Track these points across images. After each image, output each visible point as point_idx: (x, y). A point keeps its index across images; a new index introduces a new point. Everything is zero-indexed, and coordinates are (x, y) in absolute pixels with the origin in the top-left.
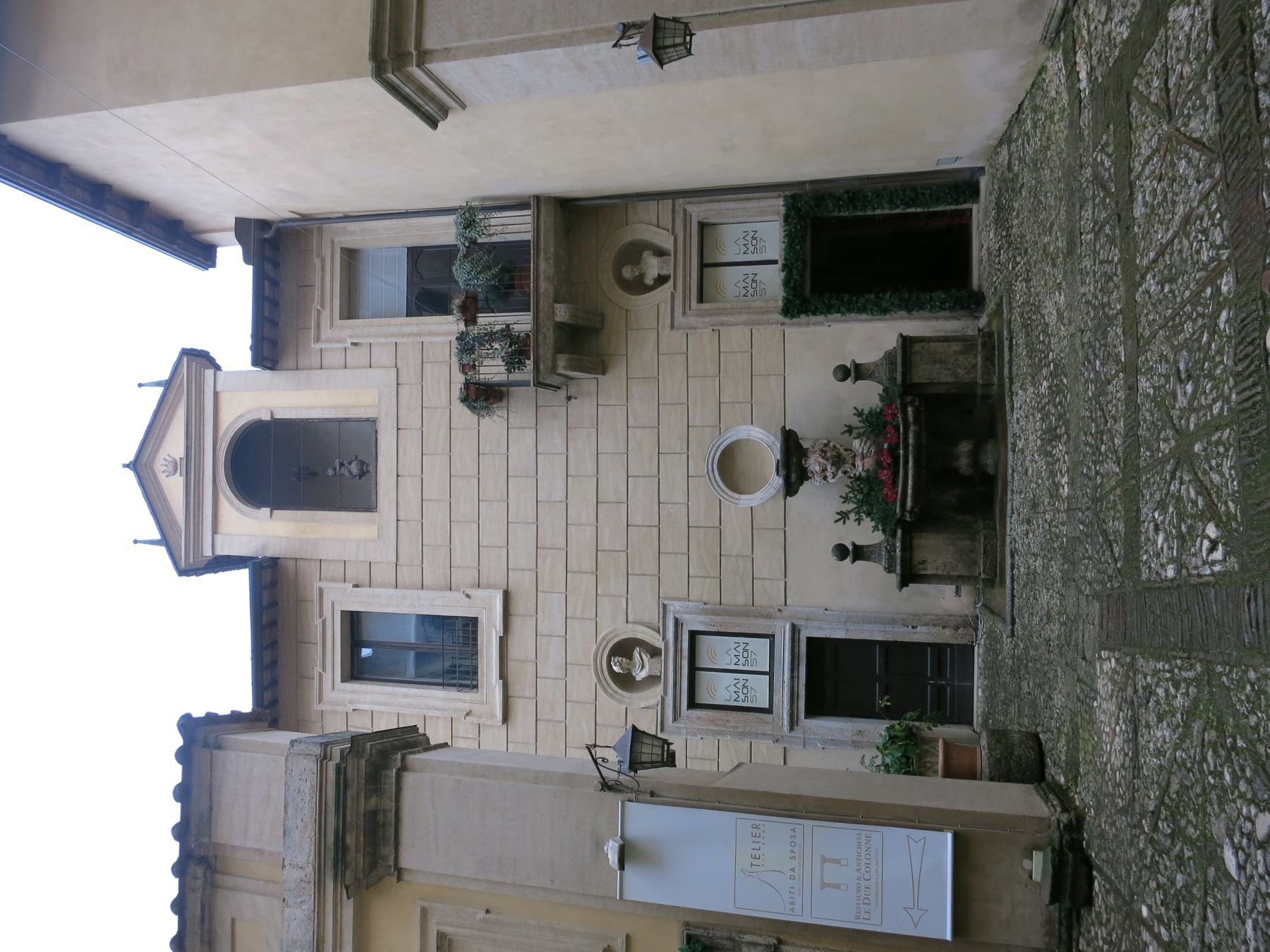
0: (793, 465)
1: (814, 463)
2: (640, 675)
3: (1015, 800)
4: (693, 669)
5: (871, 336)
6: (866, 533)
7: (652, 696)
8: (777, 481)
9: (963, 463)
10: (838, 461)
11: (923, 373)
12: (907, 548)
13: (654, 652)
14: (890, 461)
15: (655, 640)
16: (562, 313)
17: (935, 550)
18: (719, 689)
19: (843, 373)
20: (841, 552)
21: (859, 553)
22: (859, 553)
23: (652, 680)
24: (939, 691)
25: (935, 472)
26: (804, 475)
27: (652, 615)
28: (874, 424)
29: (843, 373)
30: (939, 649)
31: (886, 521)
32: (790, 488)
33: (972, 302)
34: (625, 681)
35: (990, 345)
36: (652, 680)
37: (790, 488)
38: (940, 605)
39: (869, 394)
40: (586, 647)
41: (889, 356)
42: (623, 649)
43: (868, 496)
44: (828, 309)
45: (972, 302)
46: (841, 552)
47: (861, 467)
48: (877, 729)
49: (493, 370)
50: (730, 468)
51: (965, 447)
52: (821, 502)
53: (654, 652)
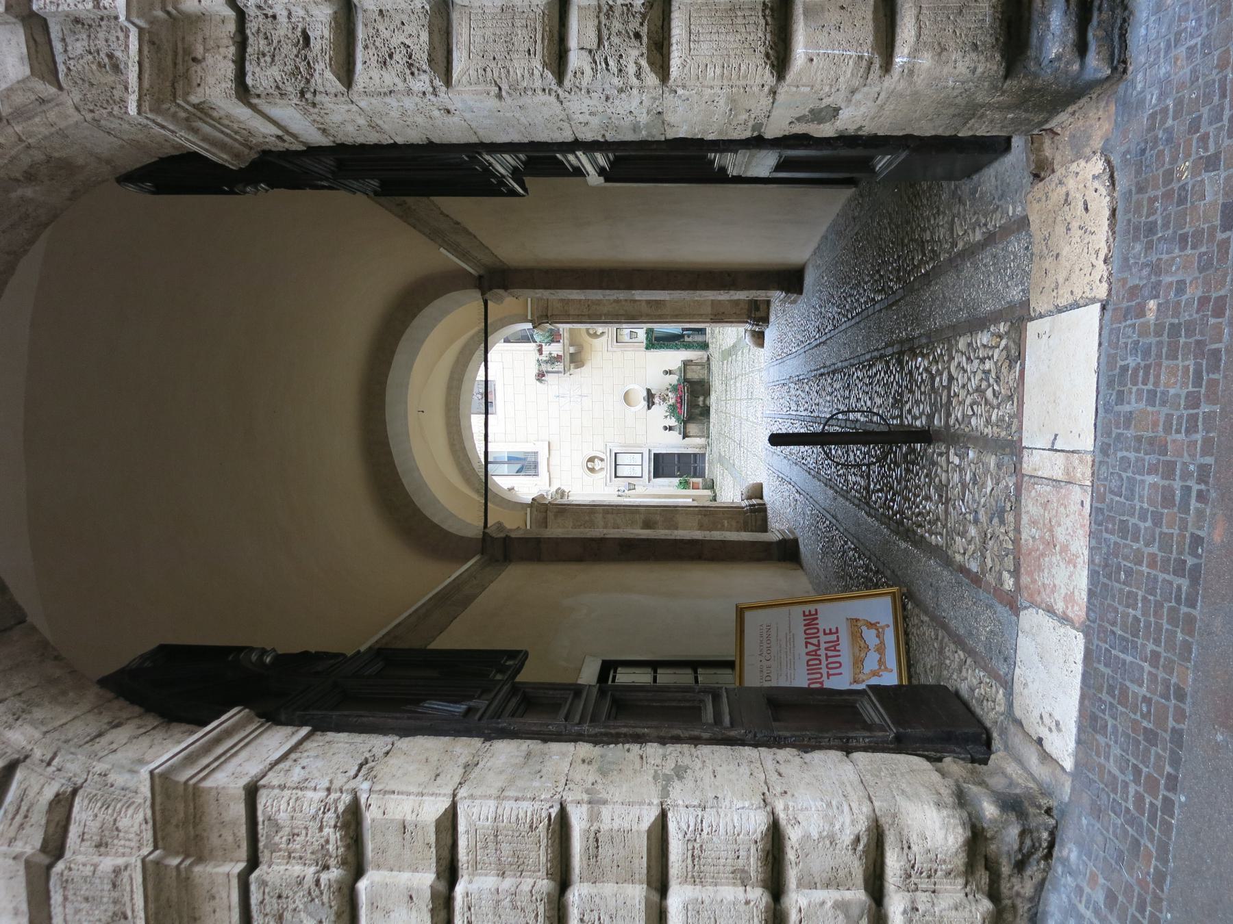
0: (650, 398)
1: (656, 400)
2: (597, 468)
3: (708, 492)
4: (616, 465)
5: (674, 358)
6: (672, 422)
7: (602, 475)
8: (645, 403)
9: (701, 404)
10: (664, 400)
11: (689, 376)
12: (685, 428)
13: (602, 460)
14: (680, 400)
15: (603, 456)
16: (572, 350)
17: (693, 428)
18: (622, 471)
19: (666, 372)
20: (665, 428)
21: (671, 428)
22: (671, 428)
23: (602, 469)
24: (695, 468)
25: (692, 405)
26: (653, 403)
27: (603, 449)
28: (675, 389)
29: (666, 372)
30: (695, 455)
31: (678, 420)
32: (649, 408)
33: (704, 346)
34: (592, 470)
35: (707, 364)
36: (602, 469)
37: (649, 408)
38: (692, 445)
39: (674, 379)
40: (580, 459)
41: (680, 369)
42: (591, 460)
43: (673, 410)
44: (661, 347)
45: (704, 346)
46: (665, 428)
47: (672, 401)
48: (676, 481)
49: (544, 368)
50: (627, 398)
51: (701, 399)
52: (660, 410)
53: (602, 460)
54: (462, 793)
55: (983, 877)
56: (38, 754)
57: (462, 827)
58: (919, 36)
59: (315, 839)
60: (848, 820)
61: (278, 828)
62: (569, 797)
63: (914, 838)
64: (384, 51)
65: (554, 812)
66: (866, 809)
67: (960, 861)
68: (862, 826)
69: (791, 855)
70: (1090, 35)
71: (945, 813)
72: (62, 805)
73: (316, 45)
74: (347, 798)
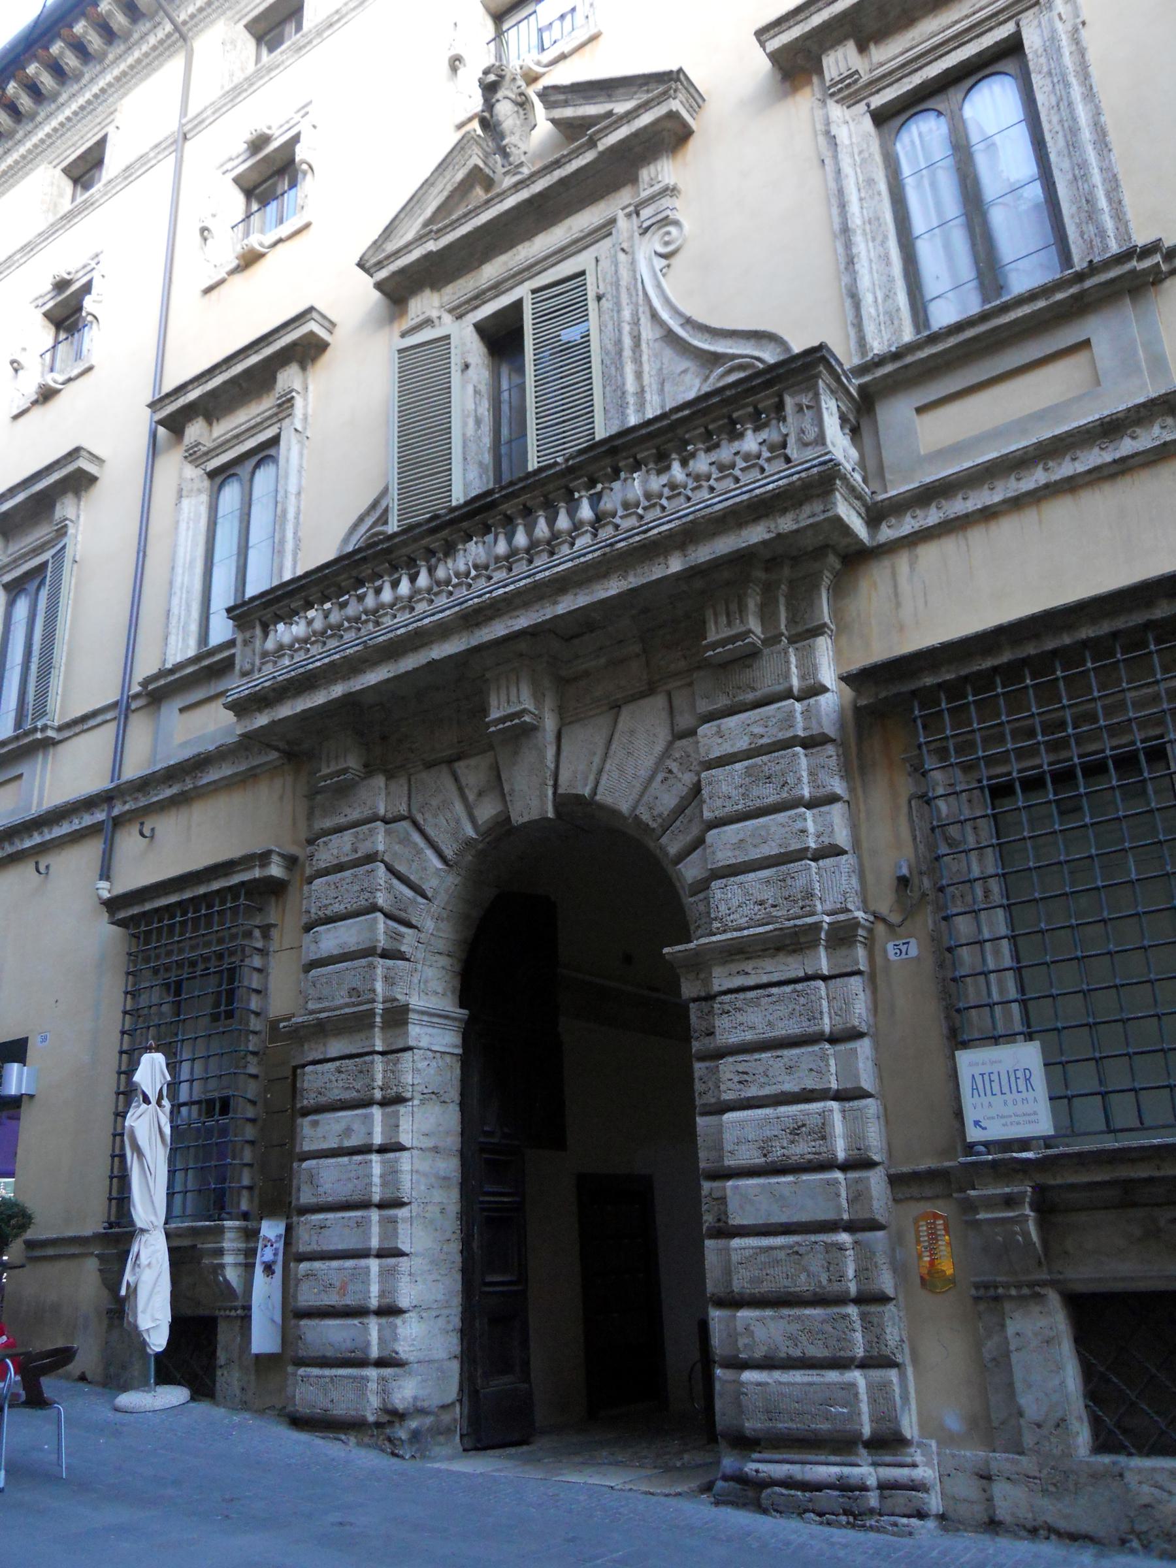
54: (415, 1152)
55: (385, 1418)
56: (422, 935)
57: (398, 1154)
58: (726, 1381)
59: (392, 1084)
60: (407, 1349)
61: (395, 1065)
62: (414, 1206)
63: (399, 1383)
64: (706, 1079)
65: (405, 1200)
66: (412, 1359)
67: (389, 1406)
68: (403, 1356)
69: (391, 1319)
70: (732, 1483)
71: (411, 1400)
72: (401, 956)
73: (707, 1040)
74: (408, 1095)
